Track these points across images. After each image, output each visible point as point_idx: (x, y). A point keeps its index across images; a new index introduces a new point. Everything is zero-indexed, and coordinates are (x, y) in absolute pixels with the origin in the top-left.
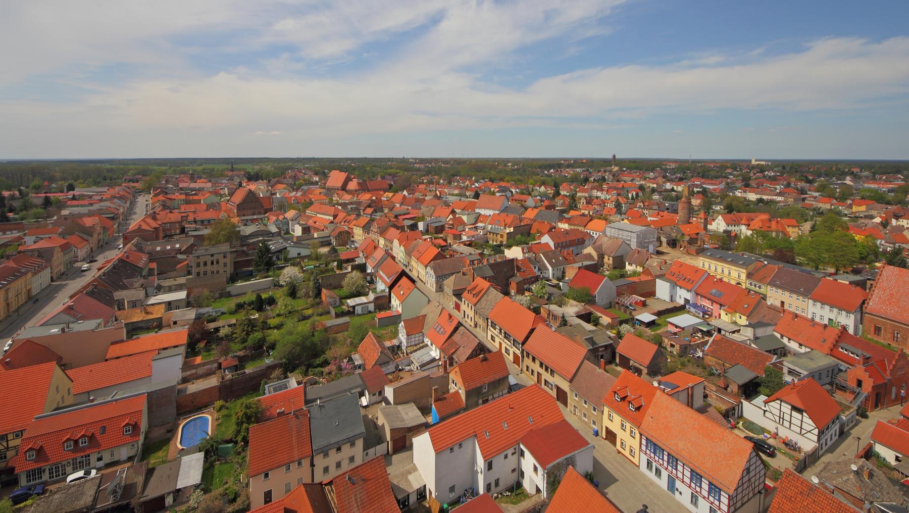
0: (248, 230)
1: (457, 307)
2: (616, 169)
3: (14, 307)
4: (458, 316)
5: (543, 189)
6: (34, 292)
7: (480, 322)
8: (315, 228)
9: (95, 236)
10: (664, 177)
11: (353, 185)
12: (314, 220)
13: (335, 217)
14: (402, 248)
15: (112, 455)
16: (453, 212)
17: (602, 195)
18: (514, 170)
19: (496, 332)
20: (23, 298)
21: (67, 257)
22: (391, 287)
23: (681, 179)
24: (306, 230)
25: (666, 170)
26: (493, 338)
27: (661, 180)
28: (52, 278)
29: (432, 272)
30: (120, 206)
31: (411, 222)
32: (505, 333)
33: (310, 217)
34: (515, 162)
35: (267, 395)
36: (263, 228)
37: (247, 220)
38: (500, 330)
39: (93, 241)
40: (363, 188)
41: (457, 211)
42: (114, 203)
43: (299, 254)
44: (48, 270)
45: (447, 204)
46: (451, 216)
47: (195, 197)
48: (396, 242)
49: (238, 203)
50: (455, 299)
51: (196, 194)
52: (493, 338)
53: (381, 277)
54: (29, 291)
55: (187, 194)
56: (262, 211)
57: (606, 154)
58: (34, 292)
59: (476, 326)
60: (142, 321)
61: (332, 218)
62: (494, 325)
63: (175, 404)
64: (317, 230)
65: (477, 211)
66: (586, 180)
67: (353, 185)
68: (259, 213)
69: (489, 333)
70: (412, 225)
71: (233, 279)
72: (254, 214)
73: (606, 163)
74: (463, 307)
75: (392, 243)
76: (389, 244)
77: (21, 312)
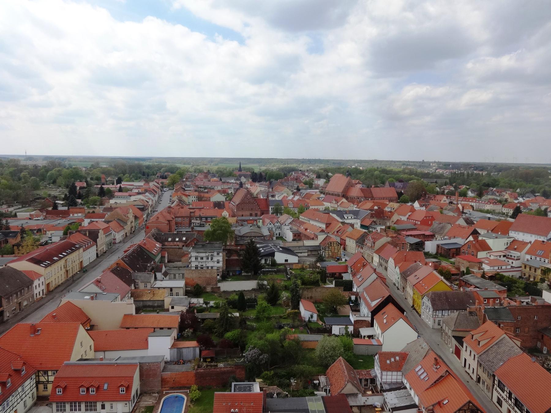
0: (245, 230)
1: (458, 353)
3: (70, 275)
4: (456, 363)
6: (85, 264)
7: (484, 376)
8: (305, 235)
9: (129, 223)
12: (305, 226)
13: (328, 225)
14: (398, 270)
15: (112, 407)
16: (475, 233)
19: (505, 395)
20: (77, 269)
21: (108, 239)
22: (375, 312)
24: (298, 236)
26: (499, 402)
28: (97, 254)
29: (429, 304)
30: (149, 199)
31: (417, 240)
32: (516, 400)
33: (302, 223)
35: (233, 392)
36: (255, 229)
37: (244, 221)
38: (510, 394)
41: (481, 231)
42: (145, 196)
43: (286, 261)
44: (94, 247)
45: (469, 222)
46: (471, 238)
47: (206, 195)
48: (391, 262)
49: (237, 203)
50: (454, 342)
51: (207, 192)
52: (499, 402)
53: (365, 299)
54: (81, 262)
56: (259, 213)
58: (85, 264)
59: (479, 380)
60: (150, 301)
61: (323, 226)
62: (501, 386)
63: (160, 379)
64: (308, 238)
65: (512, 234)
68: (256, 215)
69: (495, 394)
70: (417, 244)
71: (224, 277)
72: (251, 215)
74: (464, 354)
75: (387, 262)
76: (383, 263)
77: (75, 278)
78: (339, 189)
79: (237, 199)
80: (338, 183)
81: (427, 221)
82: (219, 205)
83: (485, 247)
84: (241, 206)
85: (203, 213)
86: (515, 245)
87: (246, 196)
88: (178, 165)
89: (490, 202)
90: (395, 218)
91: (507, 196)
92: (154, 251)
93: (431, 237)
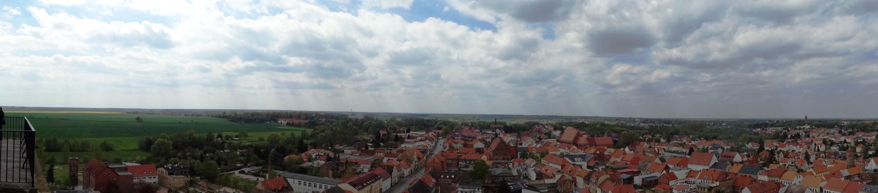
0: (499, 171)
2: (807, 127)
5: (750, 146)
10: (840, 132)
11: (583, 140)
17: (797, 149)
18: (727, 130)
23: (850, 133)
25: (841, 127)
27: (837, 134)
34: (729, 122)
39: (413, 166)
40: (591, 143)
45: (663, 160)
55: (466, 140)
57: (801, 116)
65: (690, 166)
66: (785, 136)
67: (583, 140)
68: (508, 159)
73: (801, 122)
78: (571, 139)
79: (493, 146)
80: (570, 133)
81: (635, 161)
82: (480, 151)
83: (674, 177)
84: (495, 152)
85: (468, 157)
86: (691, 174)
87: (499, 144)
88: (450, 120)
89: (675, 145)
90: (612, 160)
91: (685, 141)
92: (431, 185)
93: (638, 173)
